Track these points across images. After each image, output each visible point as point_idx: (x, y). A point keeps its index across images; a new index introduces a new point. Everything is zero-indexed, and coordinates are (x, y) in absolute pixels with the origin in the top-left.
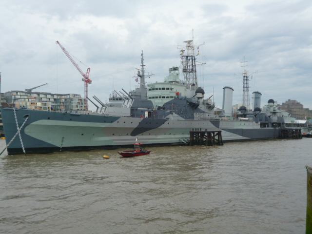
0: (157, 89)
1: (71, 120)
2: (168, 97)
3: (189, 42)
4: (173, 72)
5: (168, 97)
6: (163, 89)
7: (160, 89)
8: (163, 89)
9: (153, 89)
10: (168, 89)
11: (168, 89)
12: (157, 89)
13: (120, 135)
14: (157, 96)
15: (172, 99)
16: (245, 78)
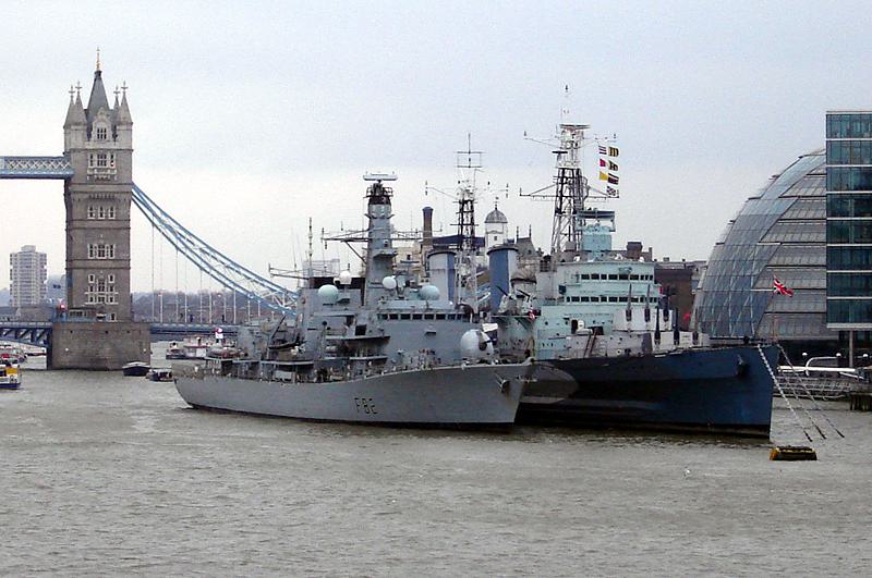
0: (636, 277)
3: (571, 128)
9: (624, 277)
12: (636, 277)
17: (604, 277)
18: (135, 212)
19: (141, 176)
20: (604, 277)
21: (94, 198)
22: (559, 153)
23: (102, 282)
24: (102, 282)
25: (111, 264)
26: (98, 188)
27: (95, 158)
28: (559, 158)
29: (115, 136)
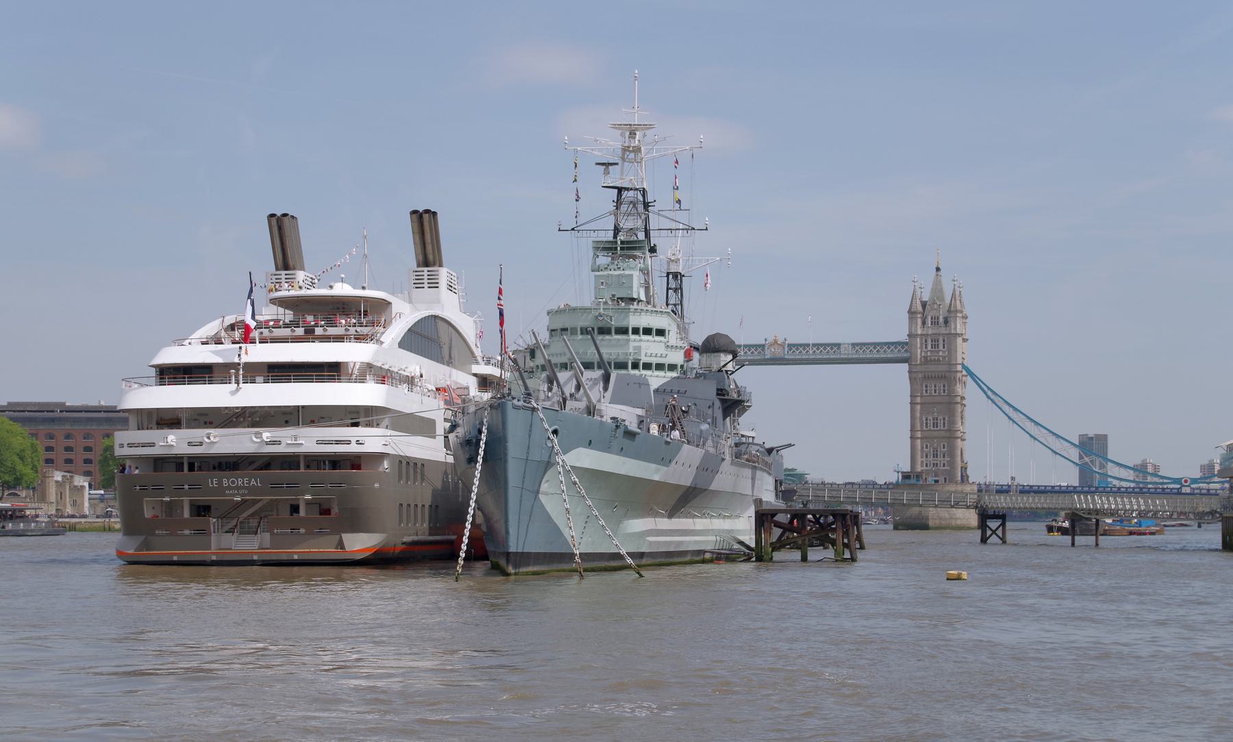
0: (623, 331)
1: (621, 451)
2: (660, 367)
4: (603, 260)
5: (660, 367)
6: (647, 331)
7: (636, 331)
8: (647, 331)
9: (604, 331)
10: (661, 332)
11: (661, 332)
12: (623, 331)
13: (656, 515)
14: (621, 359)
15: (674, 374)
16: (673, 284)
17: (573, 331)
18: (969, 392)
19: (968, 353)
20: (573, 331)
21: (927, 378)
22: (607, 165)
23: (935, 450)
24: (935, 450)
25: (943, 434)
26: (932, 368)
27: (929, 342)
28: (607, 173)
29: (946, 322)
